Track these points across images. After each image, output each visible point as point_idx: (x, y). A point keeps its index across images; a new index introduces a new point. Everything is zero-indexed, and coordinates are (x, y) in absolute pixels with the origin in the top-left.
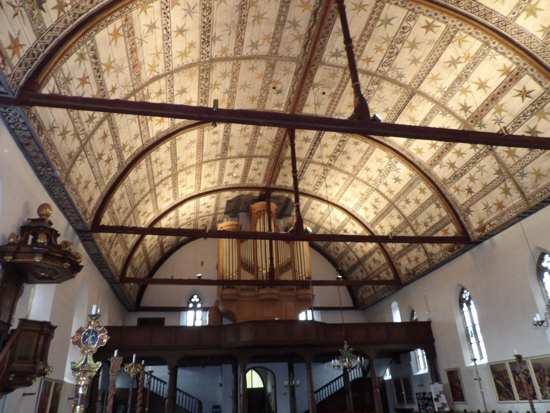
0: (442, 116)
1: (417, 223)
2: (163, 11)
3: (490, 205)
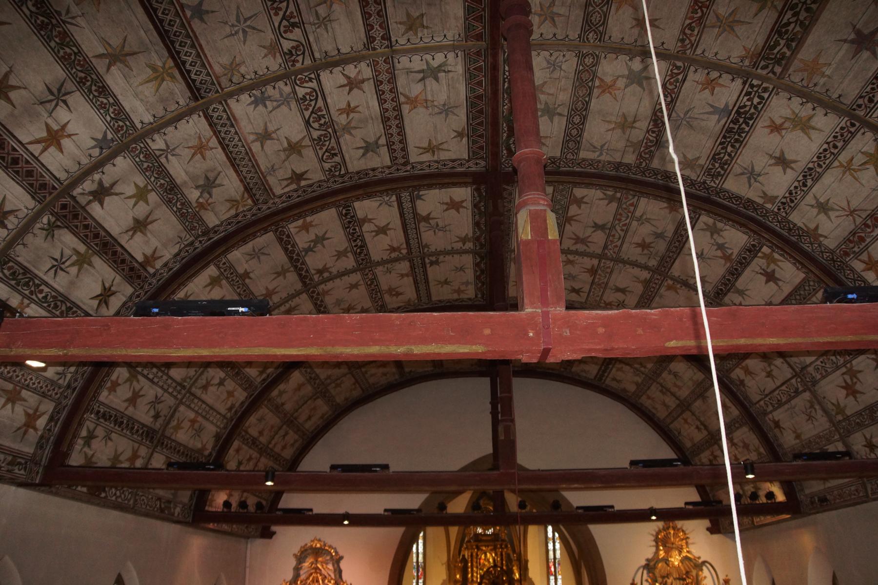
0: (100, 136)
2: (792, 205)
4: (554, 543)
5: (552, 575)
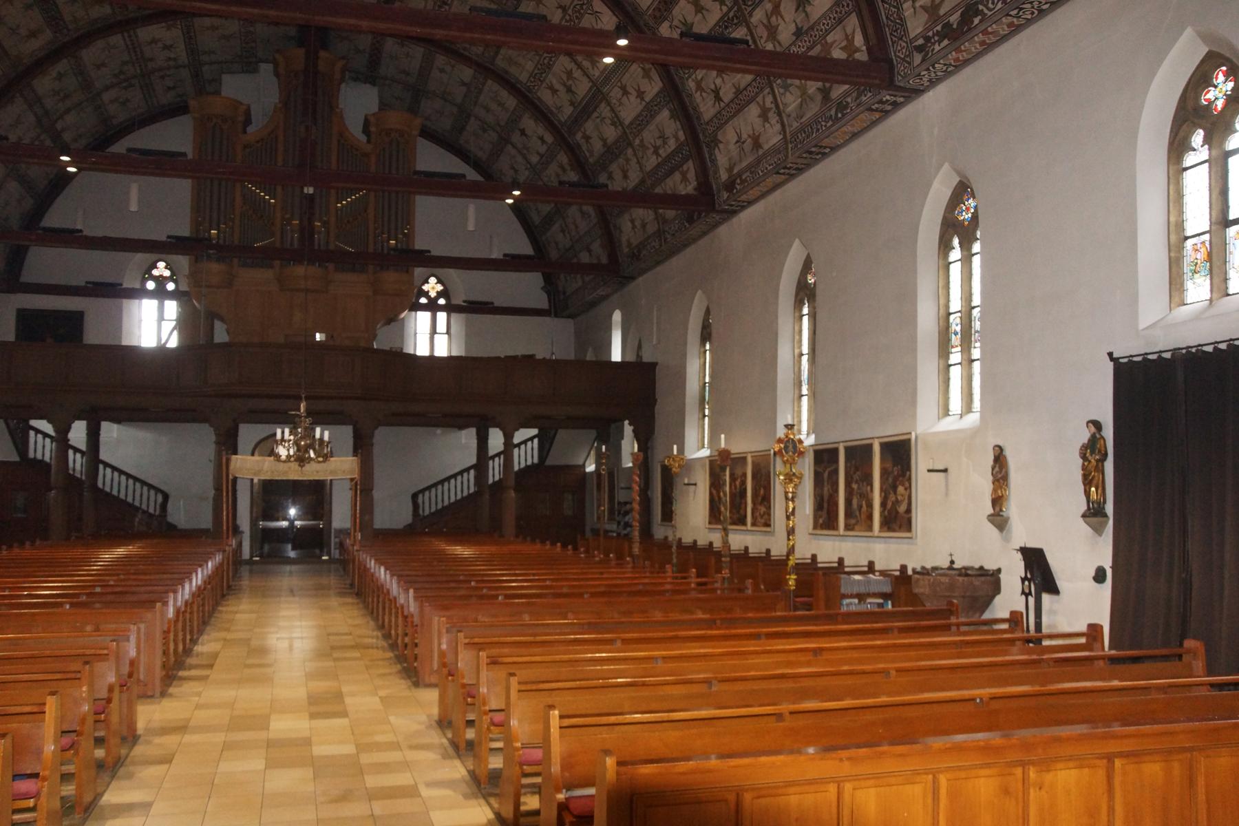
1: (642, 145)
3: (744, 136)
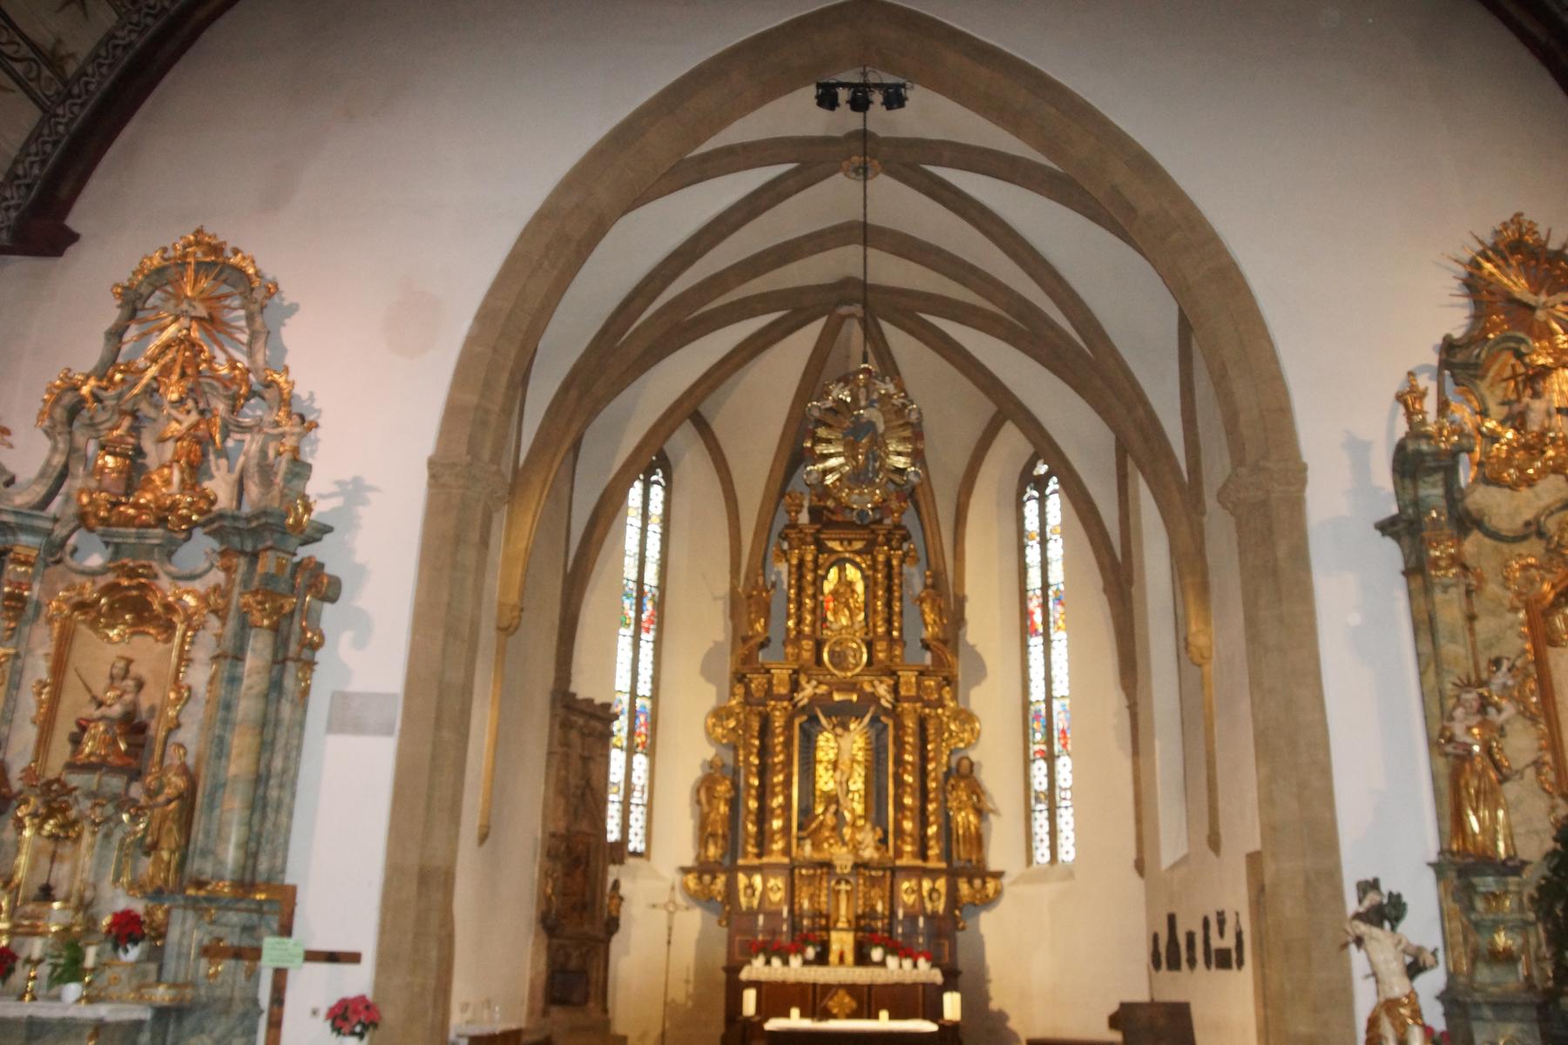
4: (1044, 542)
5: (1035, 632)
